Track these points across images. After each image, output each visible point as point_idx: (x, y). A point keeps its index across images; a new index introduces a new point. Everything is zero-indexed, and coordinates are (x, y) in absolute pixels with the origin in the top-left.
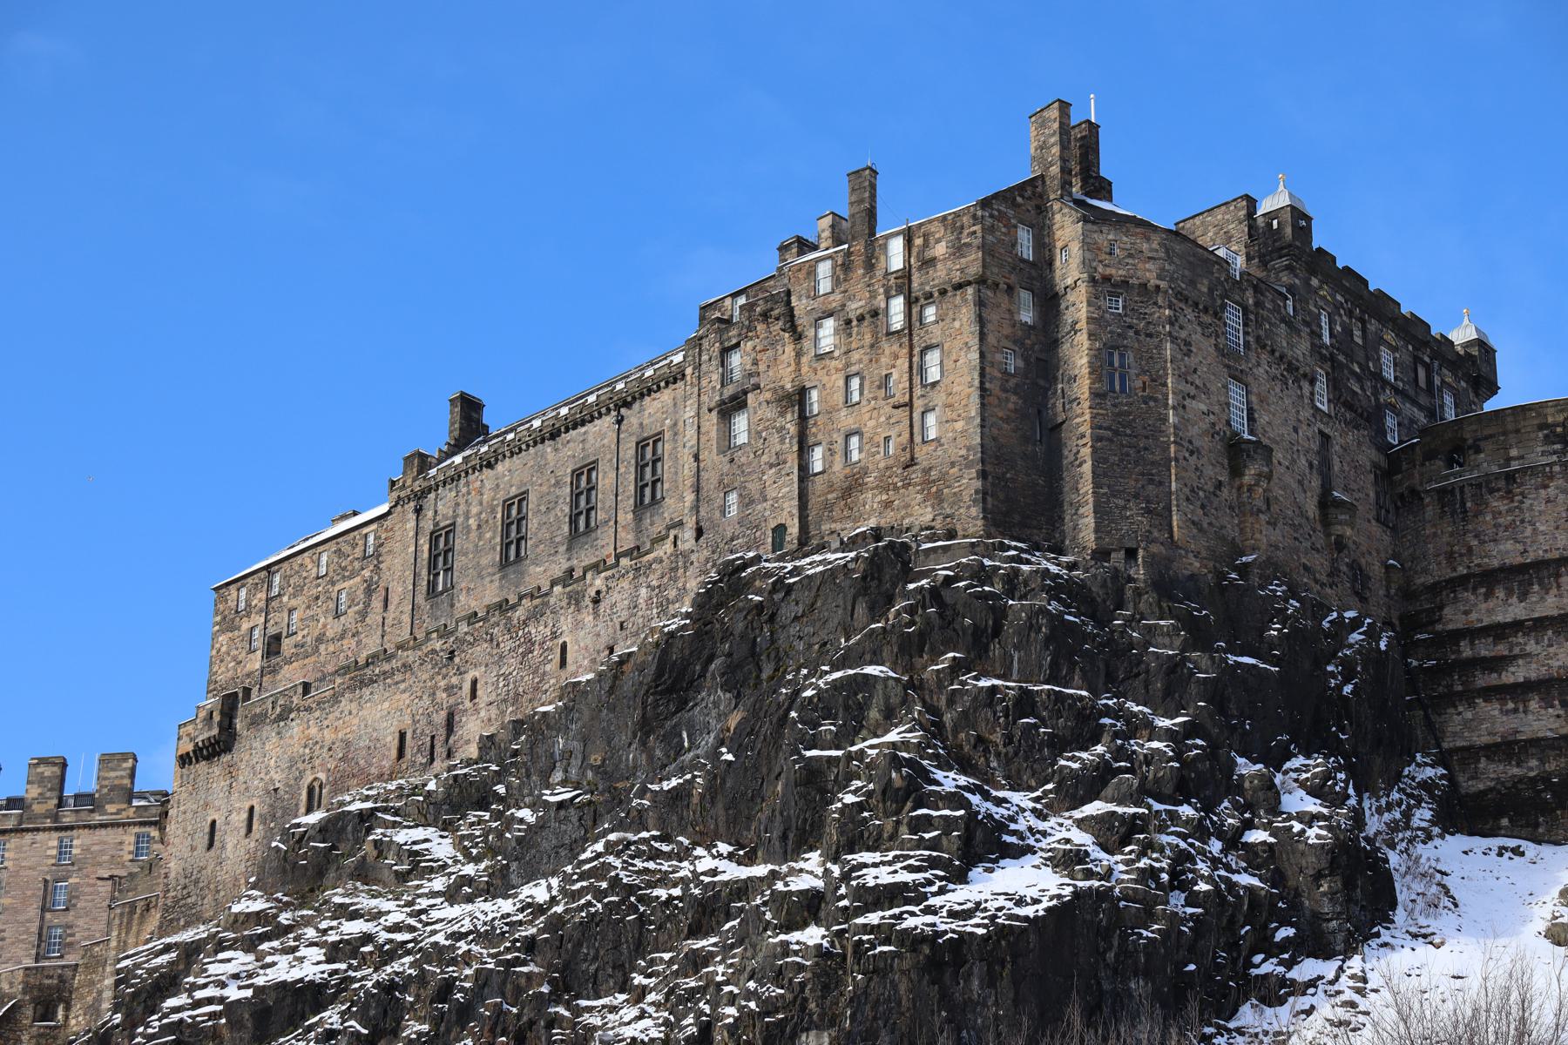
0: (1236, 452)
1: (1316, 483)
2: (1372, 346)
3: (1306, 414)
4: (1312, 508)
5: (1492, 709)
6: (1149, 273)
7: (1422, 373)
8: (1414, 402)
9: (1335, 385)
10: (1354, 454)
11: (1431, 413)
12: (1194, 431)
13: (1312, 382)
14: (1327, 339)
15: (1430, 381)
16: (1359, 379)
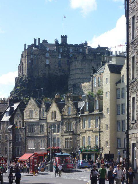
0: (46, 65)
1: (58, 65)
2: (68, 49)
3: (58, 59)
4: (57, 67)
5: (70, 81)
6: (38, 53)
7: (76, 49)
8: (74, 52)
9: (62, 56)
10: (66, 59)
11: (77, 52)
12: (41, 65)
13: (58, 56)
14: (62, 51)
15: (77, 49)
16: (65, 53)
